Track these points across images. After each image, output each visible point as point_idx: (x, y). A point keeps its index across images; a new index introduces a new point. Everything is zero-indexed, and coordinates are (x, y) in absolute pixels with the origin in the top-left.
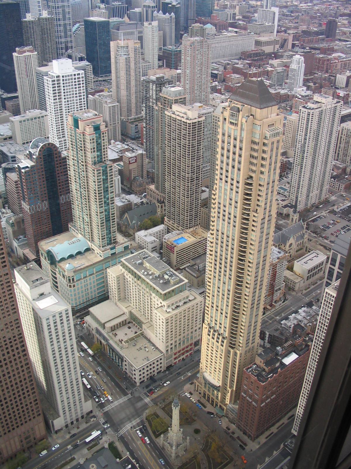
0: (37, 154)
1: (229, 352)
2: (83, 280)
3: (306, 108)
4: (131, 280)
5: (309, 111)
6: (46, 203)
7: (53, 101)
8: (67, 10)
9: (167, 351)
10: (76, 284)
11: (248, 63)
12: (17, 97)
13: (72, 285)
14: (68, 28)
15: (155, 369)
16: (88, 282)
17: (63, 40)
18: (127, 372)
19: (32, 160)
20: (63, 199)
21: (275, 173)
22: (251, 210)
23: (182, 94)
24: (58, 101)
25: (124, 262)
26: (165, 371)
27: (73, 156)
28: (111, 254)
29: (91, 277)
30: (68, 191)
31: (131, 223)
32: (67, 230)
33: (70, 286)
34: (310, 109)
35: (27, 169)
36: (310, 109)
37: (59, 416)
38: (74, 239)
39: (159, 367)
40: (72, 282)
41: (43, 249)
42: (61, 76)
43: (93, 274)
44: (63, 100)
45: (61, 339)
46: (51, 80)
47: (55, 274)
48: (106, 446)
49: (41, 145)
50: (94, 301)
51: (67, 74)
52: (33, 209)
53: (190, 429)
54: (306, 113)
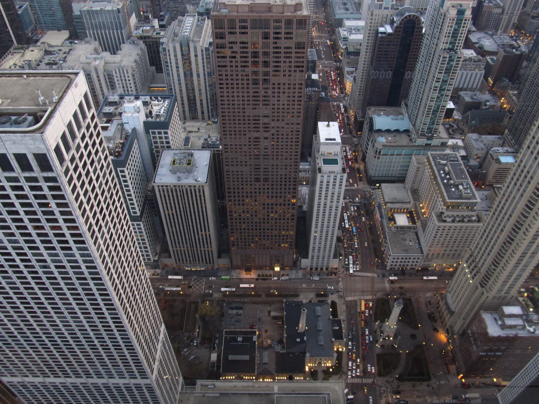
1: (477, 288)
2: (388, 157)
6: (391, 73)
9: (428, 255)
15: (410, 264)
16: (394, 160)
18: (385, 252)
20: (408, 75)
25: (430, 155)
26: (418, 270)
28: (426, 144)
29: (398, 157)
30: (413, 69)
32: (398, 105)
33: (375, 157)
35: (384, 35)
37: (307, 258)
39: (414, 264)
45: (329, 198)
48: (329, 301)
49: (407, 14)
50: (394, 179)
53: (409, 331)
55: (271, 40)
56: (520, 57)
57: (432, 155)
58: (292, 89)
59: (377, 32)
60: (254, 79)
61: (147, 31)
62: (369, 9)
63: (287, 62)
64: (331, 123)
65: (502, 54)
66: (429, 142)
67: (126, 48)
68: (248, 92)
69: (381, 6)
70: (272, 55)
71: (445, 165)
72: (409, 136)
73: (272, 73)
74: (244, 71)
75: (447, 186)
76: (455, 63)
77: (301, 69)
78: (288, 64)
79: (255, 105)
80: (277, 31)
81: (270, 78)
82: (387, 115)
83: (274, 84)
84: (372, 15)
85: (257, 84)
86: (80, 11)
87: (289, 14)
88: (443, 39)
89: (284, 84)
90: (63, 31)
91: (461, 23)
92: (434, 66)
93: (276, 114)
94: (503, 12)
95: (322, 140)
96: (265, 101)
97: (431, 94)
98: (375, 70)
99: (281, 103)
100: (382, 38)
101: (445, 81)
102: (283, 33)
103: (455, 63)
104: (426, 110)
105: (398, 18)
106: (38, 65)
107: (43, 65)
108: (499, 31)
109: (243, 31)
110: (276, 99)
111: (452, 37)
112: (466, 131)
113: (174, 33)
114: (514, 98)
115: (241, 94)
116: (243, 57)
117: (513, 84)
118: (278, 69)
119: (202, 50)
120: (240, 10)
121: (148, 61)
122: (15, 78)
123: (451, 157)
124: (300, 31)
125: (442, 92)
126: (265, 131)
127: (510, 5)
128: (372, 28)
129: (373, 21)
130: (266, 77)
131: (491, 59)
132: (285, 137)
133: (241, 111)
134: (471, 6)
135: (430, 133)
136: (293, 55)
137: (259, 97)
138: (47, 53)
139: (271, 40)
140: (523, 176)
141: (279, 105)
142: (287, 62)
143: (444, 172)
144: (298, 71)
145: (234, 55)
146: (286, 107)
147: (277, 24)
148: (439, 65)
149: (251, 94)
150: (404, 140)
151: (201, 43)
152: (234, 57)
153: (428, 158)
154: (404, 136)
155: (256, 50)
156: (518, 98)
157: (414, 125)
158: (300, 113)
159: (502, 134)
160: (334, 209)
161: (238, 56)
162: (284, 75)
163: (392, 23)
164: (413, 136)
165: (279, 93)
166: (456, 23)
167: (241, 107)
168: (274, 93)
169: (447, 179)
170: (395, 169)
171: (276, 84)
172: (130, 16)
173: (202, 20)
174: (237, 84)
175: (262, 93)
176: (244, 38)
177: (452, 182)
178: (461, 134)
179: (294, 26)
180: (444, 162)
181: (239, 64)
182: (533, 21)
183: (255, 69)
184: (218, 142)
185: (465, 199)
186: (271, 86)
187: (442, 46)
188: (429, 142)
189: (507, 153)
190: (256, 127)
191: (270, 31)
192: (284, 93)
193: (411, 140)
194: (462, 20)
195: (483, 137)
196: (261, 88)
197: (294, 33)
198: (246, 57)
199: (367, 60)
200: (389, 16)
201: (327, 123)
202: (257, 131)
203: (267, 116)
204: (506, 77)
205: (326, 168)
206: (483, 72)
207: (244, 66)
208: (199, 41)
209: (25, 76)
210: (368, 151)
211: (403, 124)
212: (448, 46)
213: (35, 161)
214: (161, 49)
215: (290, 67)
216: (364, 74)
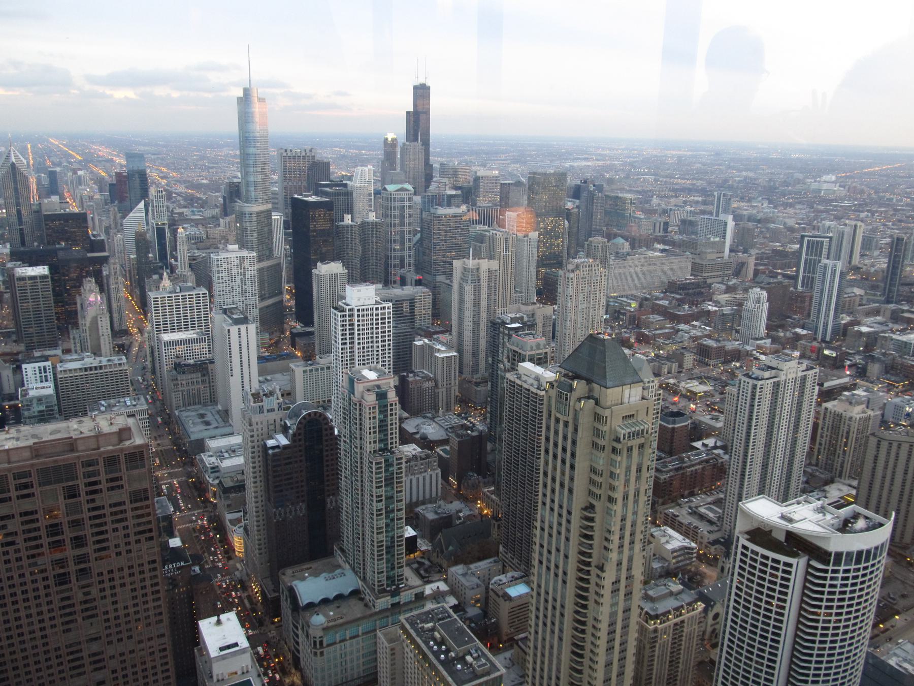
0: (295, 427)
2: (338, 646)
3: (750, 377)
4: (412, 656)
5: (755, 382)
7: (340, 347)
8: (407, 211)
10: (325, 650)
11: (678, 300)
12: (312, 333)
13: (318, 652)
14: (407, 237)
17: (398, 254)
20: (331, 502)
21: (636, 502)
22: (593, 564)
23: (542, 347)
24: (348, 346)
25: (404, 622)
28: (392, 605)
29: (354, 640)
30: (336, 491)
31: (447, 549)
32: (331, 554)
33: (315, 654)
34: (757, 379)
35: (277, 450)
36: (757, 379)
38: (338, 571)
40: (318, 646)
41: (284, 583)
42: (356, 309)
43: (357, 636)
44: (357, 346)
46: (340, 314)
49: (305, 413)
51: (365, 307)
52: (280, 514)
54: (750, 385)
55: (83, 498)
56: (481, 439)
57: (407, 619)
58: (137, 574)
59: (265, 448)
60: (59, 575)
62: (244, 416)
63: (120, 529)
64: (223, 617)
65: (455, 440)
66: (396, 600)
70: (88, 523)
71: (433, 629)
72: (362, 599)
73: (93, 556)
74: (35, 564)
75: (448, 664)
76: (395, 467)
77: (148, 535)
78: (121, 533)
79: (67, 623)
81: (91, 564)
82: (316, 574)
84: (250, 425)
85: (65, 583)
87: (111, 448)
88: (368, 438)
89: (121, 569)
91: (387, 411)
92: (366, 479)
93: (114, 630)
94: (437, 385)
95: (213, 652)
96: (87, 610)
97: (375, 522)
98: (277, 508)
99: (120, 606)
100: (274, 455)
101: (390, 498)
102: (104, 481)
103: (395, 467)
104: (375, 549)
105: (292, 422)
108: (441, 411)
109: (25, 492)
110: (109, 600)
111: (380, 431)
112: (445, 565)
114: (493, 497)
115: (34, 611)
116: (30, 539)
117: (484, 477)
118: (104, 545)
120: (14, 459)
123: (437, 614)
124: (136, 472)
125: (391, 516)
126: (96, 669)
127: (443, 373)
128: (256, 444)
129: (255, 433)
130: (82, 566)
131: (444, 451)
132: (139, 668)
133: (39, 642)
134: (392, 385)
135: (393, 585)
136: (130, 514)
137: (73, 605)
139: (83, 498)
140: (550, 607)
141: (116, 610)
142: (120, 529)
143: (436, 643)
144: (143, 540)
145: (10, 539)
146: (131, 610)
147: (91, 469)
148: (374, 475)
149: (56, 604)
150: (355, 609)
152: (12, 543)
153: (403, 627)
154: (353, 601)
155: (56, 521)
156: (499, 495)
157: (364, 579)
158: (161, 614)
159: (497, 553)
161: (19, 539)
162: (118, 554)
163: (285, 430)
164: (367, 598)
166: (380, 412)
167: (38, 634)
169: (443, 652)
170: (355, 663)
171: (105, 572)
175: (80, 596)
176: (27, 505)
177: (453, 654)
178: (440, 572)
179: (123, 466)
180: (430, 625)
181: (23, 554)
182: (479, 388)
183: (58, 556)
185: (482, 676)
186: (95, 579)
187: (369, 448)
188: (396, 600)
189: (514, 581)
190: (74, 668)
191: (79, 482)
193: (366, 605)
194: (386, 406)
195: (472, 566)
196: (75, 589)
197: (125, 478)
199: (259, 494)
200: (278, 421)
201: (215, 618)
202: (80, 674)
203: (96, 639)
204: (472, 470)
206: (439, 471)
207: (33, 556)
210: (301, 648)
211: (346, 582)
212: (377, 446)
215: (127, 536)
216: (261, 518)
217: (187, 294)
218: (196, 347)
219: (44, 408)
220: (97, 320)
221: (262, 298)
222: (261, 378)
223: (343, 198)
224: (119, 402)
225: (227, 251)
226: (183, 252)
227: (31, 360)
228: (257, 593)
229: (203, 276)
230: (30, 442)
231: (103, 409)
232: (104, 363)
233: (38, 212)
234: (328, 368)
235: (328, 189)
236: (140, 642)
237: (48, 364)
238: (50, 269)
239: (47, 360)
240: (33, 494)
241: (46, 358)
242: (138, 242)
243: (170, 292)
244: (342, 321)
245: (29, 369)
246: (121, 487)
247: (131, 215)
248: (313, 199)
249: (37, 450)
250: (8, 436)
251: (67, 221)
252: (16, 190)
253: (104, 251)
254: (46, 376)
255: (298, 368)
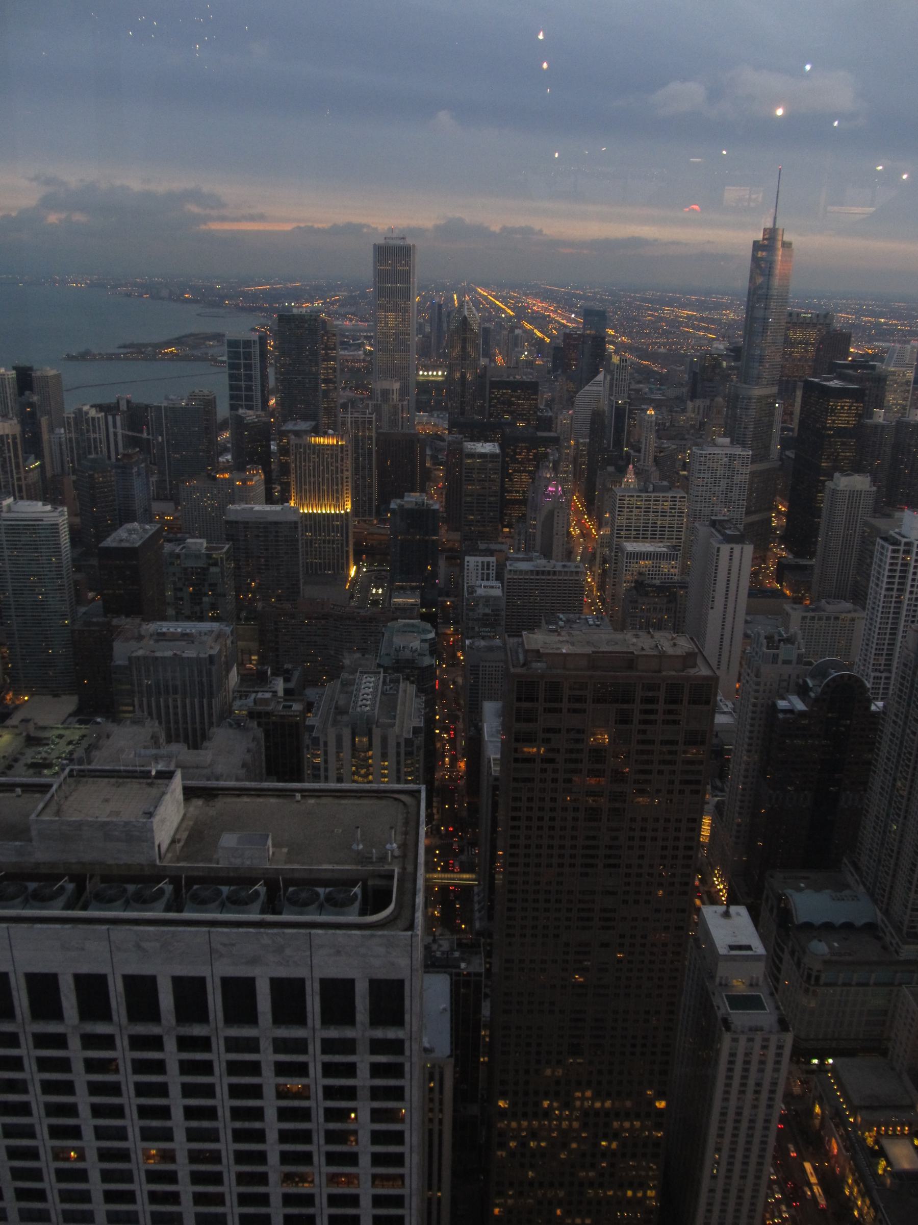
0: (819, 690)
7: (883, 592)
19: (803, 701)
24: (895, 593)
27: (896, 715)
35: (788, 716)
38: (847, 892)
40: (813, 982)
46: (891, 547)
47: (782, 950)
61: (266, 701)
64: (733, 909)
67: (221, 736)
68: (574, 838)
69: (775, 658)
72: (879, 938)
80: (649, 707)
83: (633, 820)
84: (757, 676)
86: (130, 658)
87: (674, 673)
90: (64, 698)
95: (722, 950)
96: (609, 857)
106: (10, 767)
107: (20, 768)
109: (577, 706)
113: (336, 708)
119: (398, 744)
121: (264, 764)
122: (273, 800)
138: (32, 741)
151: (397, 729)
152: (552, 761)
157: (886, 913)
160: (760, 1124)
163: (803, 691)
165: (643, 839)
168: (632, 838)
172: (228, 671)
173: (391, 681)
174: (552, 819)
184: (457, 954)
192: (654, 839)
193: (885, 948)
198: (576, 761)
205: (741, 1018)
208: (394, 725)
209: (298, 796)
211: (859, 910)
213: (317, 999)
214: (307, 740)
215: (671, 782)
217: (661, 495)
218: (665, 567)
219: (490, 612)
220: (553, 515)
221: (748, 513)
222: (748, 619)
223: (869, 385)
224: (579, 618)
225: (715, 445)
226: (650, 441)
227: (475, 552)
228: (721, 890)
229: (670, 472)
230: (589, 650)
231: (561, 623)
232: (558, 569)
233: (482, 376)
234: (837, 618)
235: (850, 372)
236: (657, 911)
237: (492, 559)
238: (501, 447)
239: (492, 555)
240: (585, 711)
241: (491, 553)
242: (593, 422)
243: (641, 491)
244: (893, 558)
245: (472, 561)
246: (676, 722)
247: (587, 388)
248: (835, 384)
249: (594, 661)
250: (561, 639)
251: (514, 391)
252: (464, 348)
253: (550, 431)
254: (488, 574)
255: (796, 615)
